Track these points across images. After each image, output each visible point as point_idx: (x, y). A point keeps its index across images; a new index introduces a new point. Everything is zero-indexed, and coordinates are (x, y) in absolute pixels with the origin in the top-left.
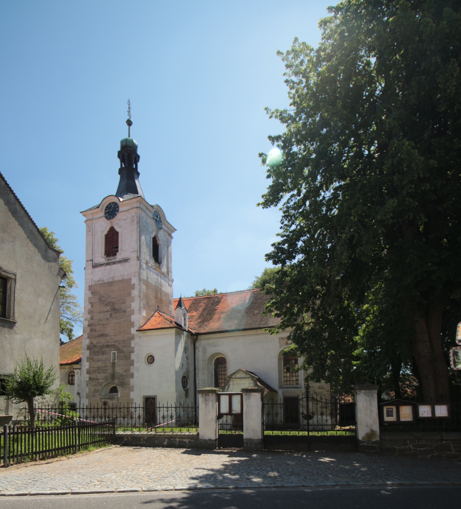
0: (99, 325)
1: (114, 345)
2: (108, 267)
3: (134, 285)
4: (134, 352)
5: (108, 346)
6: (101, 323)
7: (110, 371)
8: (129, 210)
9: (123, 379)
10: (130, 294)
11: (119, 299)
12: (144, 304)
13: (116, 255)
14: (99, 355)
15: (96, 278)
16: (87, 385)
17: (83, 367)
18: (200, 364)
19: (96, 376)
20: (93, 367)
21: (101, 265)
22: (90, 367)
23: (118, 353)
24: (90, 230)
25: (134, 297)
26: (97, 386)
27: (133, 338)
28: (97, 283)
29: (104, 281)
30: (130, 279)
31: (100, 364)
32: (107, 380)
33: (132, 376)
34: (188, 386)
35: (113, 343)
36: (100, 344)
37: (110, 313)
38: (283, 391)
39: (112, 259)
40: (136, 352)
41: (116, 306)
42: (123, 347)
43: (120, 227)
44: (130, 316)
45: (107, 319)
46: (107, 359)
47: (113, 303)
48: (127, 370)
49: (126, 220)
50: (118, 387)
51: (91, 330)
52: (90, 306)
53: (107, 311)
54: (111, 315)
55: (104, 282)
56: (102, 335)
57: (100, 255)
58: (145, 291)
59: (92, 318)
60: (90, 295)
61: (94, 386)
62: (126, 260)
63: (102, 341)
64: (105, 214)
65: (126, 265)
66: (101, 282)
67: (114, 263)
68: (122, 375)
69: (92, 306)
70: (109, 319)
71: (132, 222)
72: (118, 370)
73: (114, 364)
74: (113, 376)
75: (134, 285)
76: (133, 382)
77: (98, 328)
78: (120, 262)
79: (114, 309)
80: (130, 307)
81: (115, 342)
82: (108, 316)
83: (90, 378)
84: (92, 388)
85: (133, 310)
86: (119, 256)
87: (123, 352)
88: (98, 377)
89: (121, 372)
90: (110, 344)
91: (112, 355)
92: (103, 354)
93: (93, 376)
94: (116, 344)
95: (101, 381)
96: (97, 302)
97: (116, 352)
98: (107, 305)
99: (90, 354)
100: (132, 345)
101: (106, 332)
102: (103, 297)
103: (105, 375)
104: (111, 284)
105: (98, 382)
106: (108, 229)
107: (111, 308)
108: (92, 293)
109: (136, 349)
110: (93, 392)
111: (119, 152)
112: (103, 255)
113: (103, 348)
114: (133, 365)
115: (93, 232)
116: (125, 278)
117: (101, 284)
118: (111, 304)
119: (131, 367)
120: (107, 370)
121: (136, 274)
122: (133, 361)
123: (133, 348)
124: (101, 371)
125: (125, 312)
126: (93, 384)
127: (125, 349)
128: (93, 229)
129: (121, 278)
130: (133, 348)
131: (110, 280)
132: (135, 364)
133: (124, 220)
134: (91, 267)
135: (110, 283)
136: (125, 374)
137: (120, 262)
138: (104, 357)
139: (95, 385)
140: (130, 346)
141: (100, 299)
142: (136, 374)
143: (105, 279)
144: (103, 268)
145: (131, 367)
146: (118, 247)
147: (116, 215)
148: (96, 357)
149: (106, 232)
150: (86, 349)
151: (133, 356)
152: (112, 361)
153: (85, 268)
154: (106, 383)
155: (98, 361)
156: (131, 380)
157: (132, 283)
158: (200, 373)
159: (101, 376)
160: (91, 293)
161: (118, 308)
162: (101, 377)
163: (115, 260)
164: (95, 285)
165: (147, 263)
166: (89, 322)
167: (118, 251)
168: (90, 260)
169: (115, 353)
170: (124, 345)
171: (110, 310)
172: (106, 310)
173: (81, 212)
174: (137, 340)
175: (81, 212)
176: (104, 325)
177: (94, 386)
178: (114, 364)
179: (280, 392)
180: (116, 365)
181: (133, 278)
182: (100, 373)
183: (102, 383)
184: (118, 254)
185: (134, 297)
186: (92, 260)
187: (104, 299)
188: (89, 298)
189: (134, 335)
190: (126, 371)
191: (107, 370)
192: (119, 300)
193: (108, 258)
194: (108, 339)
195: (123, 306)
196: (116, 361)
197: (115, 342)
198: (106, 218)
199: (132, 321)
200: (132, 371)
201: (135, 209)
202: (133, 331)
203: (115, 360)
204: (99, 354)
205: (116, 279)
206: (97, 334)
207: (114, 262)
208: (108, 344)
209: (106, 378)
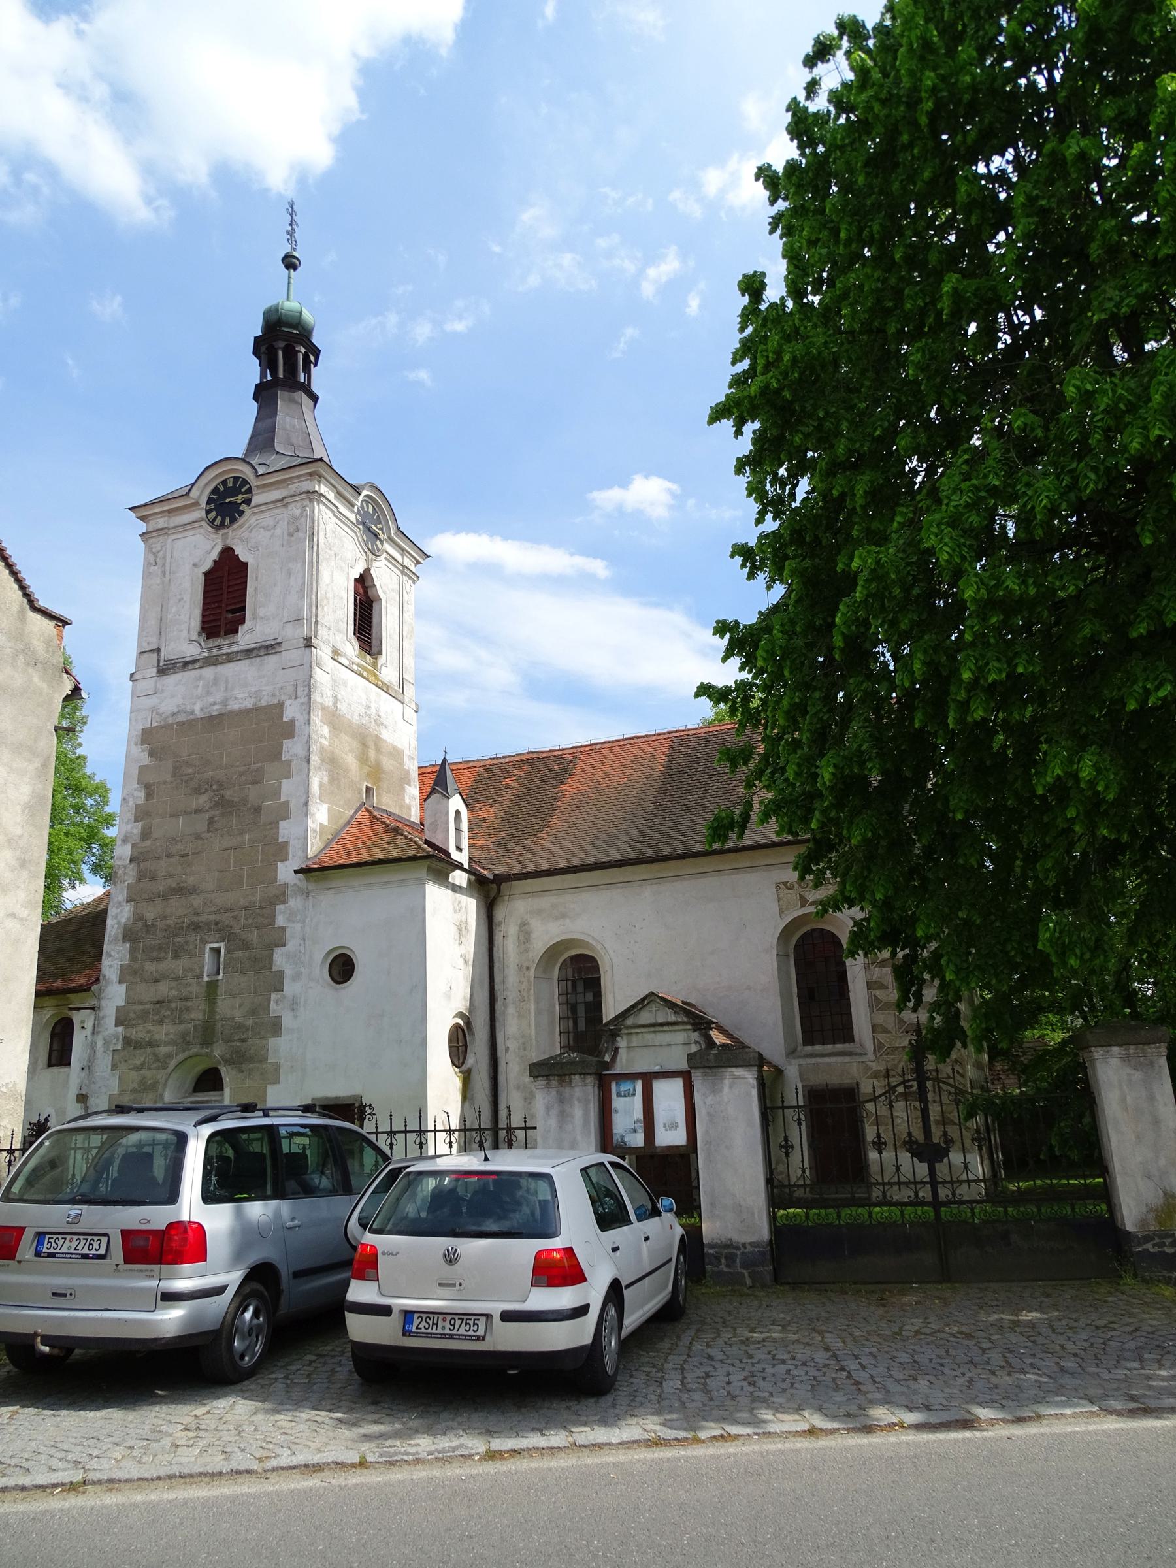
0: (169, 855)
1: (217, 923)
2: (209, 672)
3: (292, 722)
4: (284, 945)
5: (196, 927)
6: (173, 850)
7: (198, 1015)
8: (282, 499)
9: (244, 1041)
10: (276, 755)
11: (242, 769)
12: (321, 785)
13: (237, 631)
14: (161, 960)
15: (168, 706)
16: (114, 1067)
17: (103, 1003)
18: (511, 980)
19: (149, 1032)
20: (141, 1003)
21: (186, 664)
22: (129, 1001)
23: (227, 950)
24: (156, 564)
25: (289, 762)
26: (149, 1069)
27: (282, 896)
28: (171, 720)
29: (192, 713)
30: (280, 706)
31: (164, 990)
32: (188, 1044)
33: (275, 1027)
34: (470, 1061)
35: (213, 917)
36: (170, 922)
37: (207, 816)
38: (800, 1065)
39: (227, 645)
40: (292, 945)
41: (228, 793)
42: (248, 928)
43: (255, 549)
44: (274, 825)
45: (198, 837)
46: (192, 970)
47: (221, 785)
48: (259, 1009)
49: (274, 527)
50: (223, 1070)
51: (141, 876)
52: (142, 794)
53: (197, 811)
54: (211, 822)
55: (192, 717)
56: (180, 890)
57: (185, 634)
58: (326, 743)
59: (145, 835)
60: (145, 759)
61: (138, 1068)
62: (270, 648)
63: (177, 908)
64: (208, 512)
65: (272, 660)
66: (183, 718)
67: (231, 658)
68: (240, 1027)
69: (149, 795)
70: (204, 835)
71: (291, 535)
72: (229, 1008)
73: (212, 986)
74: (207, 1033)
75: (292, 722)
76: (280, 1048)
77: (162, 866)
78: (249, 653)
79: (223, 804)
80: (277, 793)
81: (219, 912)
82: (201, 824)
83: (127, 1042)
84: (133, 1075)
85: (287, 804)
86: (246, 637)
87: (246, 946)
88: (157, 1037)
89: (237, 1016)
90: (203, 918)
91: (207, 956)
92: (176, 956)
93: (139, 1033)
94: (226, 919)
95: (163, 1050)
96: (165, 783)
97: (222, 945)
98: (198, 791)
99: (133, 958)
100: (280, 921)
101: (191, 880)
102: (188, 764)
103: (182, 1027)
104: (215, 722)
105: (154, 1054)
106: (214, 555)
107: (210, 800)
108: (151, 754)
109: (294, 931)
110: (134, 1091)
111: (258, 341)
112: (195, 636)
113: (178, 935)
114: (279, 989)
115: (164, 565)
116: (263, 703)
117: (182, 724)
118: (214, 787)
119: (274, 996)
120: (188, 1009)
121: (300, 689)
122: (281, 974)
123: (284, 929)
124: (168, 1013)
125: (257, 810)
126: (138, 1062)
127: (254, 937)
128: (164, 558)
129: (248, 704)
130: (284, 929)
131: (216, 710)
132: (289, 988)
133: (266, 528)
134: (155, 670)
135: (211, 718)
136: (249, 1022)
137: (249, 653)
138: (180, 965)
139: (142, 1065)
140: (272, 924)
141: (176, 771)
142: (287, 1021)
143: (197, 708)
144: (191, 674)
145: (274, 996)
146: (243, 609)
147: (241, 513)
148: (151, 967)
149: (208, 565)
150: (120, 937)
151: (280, 958)
152: (206, 979)
153: (132, 675)
154: (181, 1057)
155: (157, 981)
156: (272, 1042)
157: (285, 719)
158: (511, 1010)
159: (164, 1032)
160: (146, 754)
161: (236, 799)
162: (167, 1034)
163: (234, 649)
164: (162, 727)
165: (336, 654)
166: (134, 845)
167: (242, 621)
168: (152, 651)
169: (218, 951)
170: (250, 921)
171: (208, 805)
172: (194, 806)
173: (130, 509)
174: (295, 903)
175: (130, 509)
176: (187, 855)
177: (138, 1068)
178: (212, 986)
179: (792, 1072)
180: (222, 990)
181: (288, 703)
182: (161, 1022)
183: (169, 1056)
184: (242, 629)
185: (289, 762)
186: (159, 650)
187: (190, 770)
188: (142, 769)
189: (285, 885)
190: (253, 1012)
191: (188, 1009)
192: (240, 774)
193: (210, 641)
194: (196, 901)
195: (253, 793)
196: (221, 977)
197: (219, 912)
198: (212, 522)
199: (281, 840)
200: (275, 1009)
201: (304, 496)
202: (285, 872)
203: (218, 973)
204: (162, 955)
205: (234, 706)
206: (160, 887)
207: (228, 654)
208: (196, 919)
209: (183, 1042)
